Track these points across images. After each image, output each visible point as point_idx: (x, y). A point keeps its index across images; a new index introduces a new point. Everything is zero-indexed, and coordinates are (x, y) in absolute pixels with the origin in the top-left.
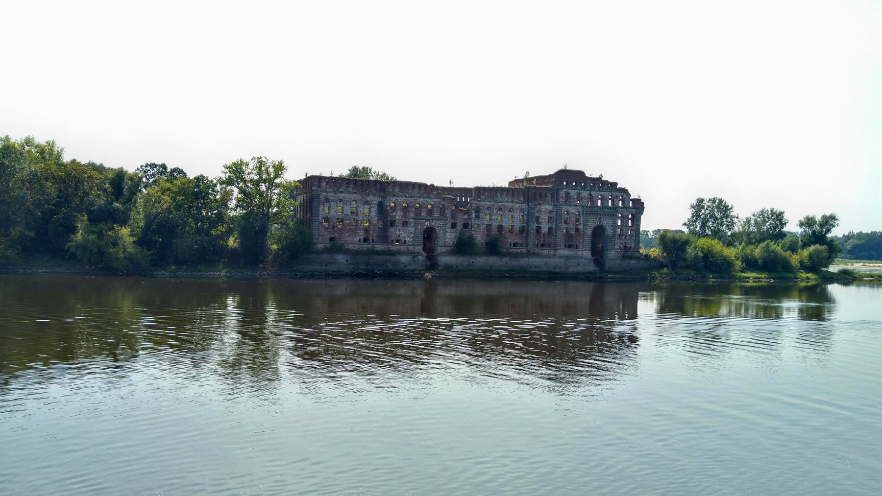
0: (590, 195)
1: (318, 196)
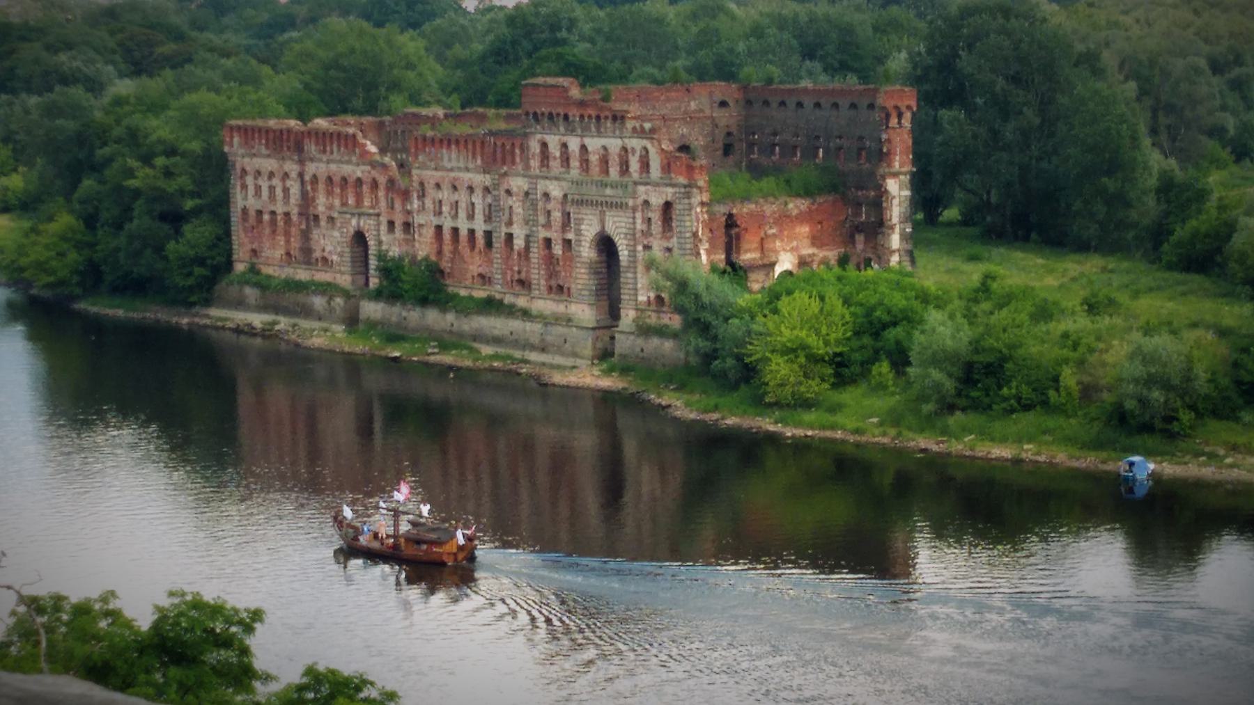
0: (584, 148)
1: (234, 165)
